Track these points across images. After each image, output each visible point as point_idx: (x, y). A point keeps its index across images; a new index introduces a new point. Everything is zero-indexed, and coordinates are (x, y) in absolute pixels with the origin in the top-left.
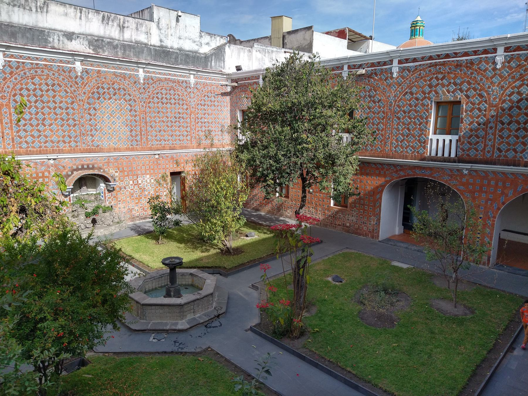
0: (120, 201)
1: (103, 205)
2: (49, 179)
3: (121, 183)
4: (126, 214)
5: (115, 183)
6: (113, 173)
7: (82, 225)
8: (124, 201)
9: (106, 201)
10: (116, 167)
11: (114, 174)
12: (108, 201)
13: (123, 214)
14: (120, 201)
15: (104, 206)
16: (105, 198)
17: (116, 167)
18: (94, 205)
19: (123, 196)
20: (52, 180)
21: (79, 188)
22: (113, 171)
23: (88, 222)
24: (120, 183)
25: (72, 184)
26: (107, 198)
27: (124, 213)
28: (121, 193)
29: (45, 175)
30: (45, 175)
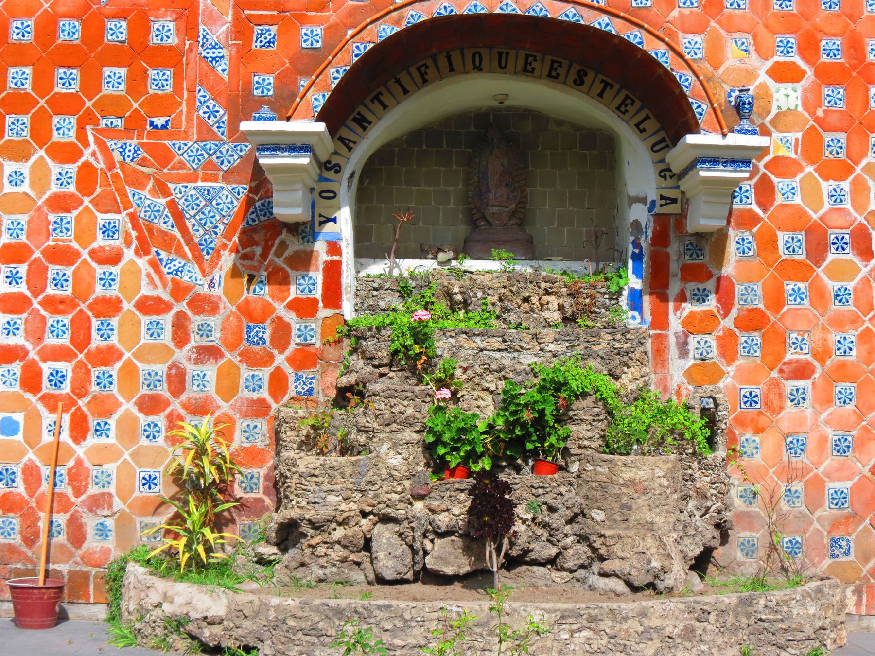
0: (802, 371)
1: (628, 381)
2: (178, 78)
3: (827, 186)
4: (854, 518)
5: (735, 139)
6: (752, 75)
7: (384, 535)
8: (842, 372)
9: (660, 351)
10: (789, 23)
11: (766, 95)
12: (683, 352)
13: (826, 511)
14: (802, 371)
15: (637, 397)
16: (660, 321)
17: (789, 23)
18: (528, 359)
19: (839, 323)
20: (202, 93)
21: (462, 230)
22: (754, 59)
23: (443, 520)
24: (811, 193)
25: (318, 99)
26: (675, 323)
27: (838, 499)
28: (818, 295)
29: (154, 41)
30: (154, 41)
